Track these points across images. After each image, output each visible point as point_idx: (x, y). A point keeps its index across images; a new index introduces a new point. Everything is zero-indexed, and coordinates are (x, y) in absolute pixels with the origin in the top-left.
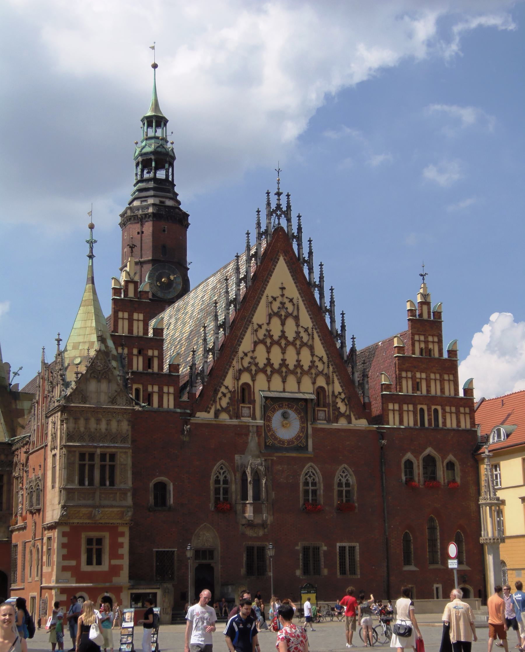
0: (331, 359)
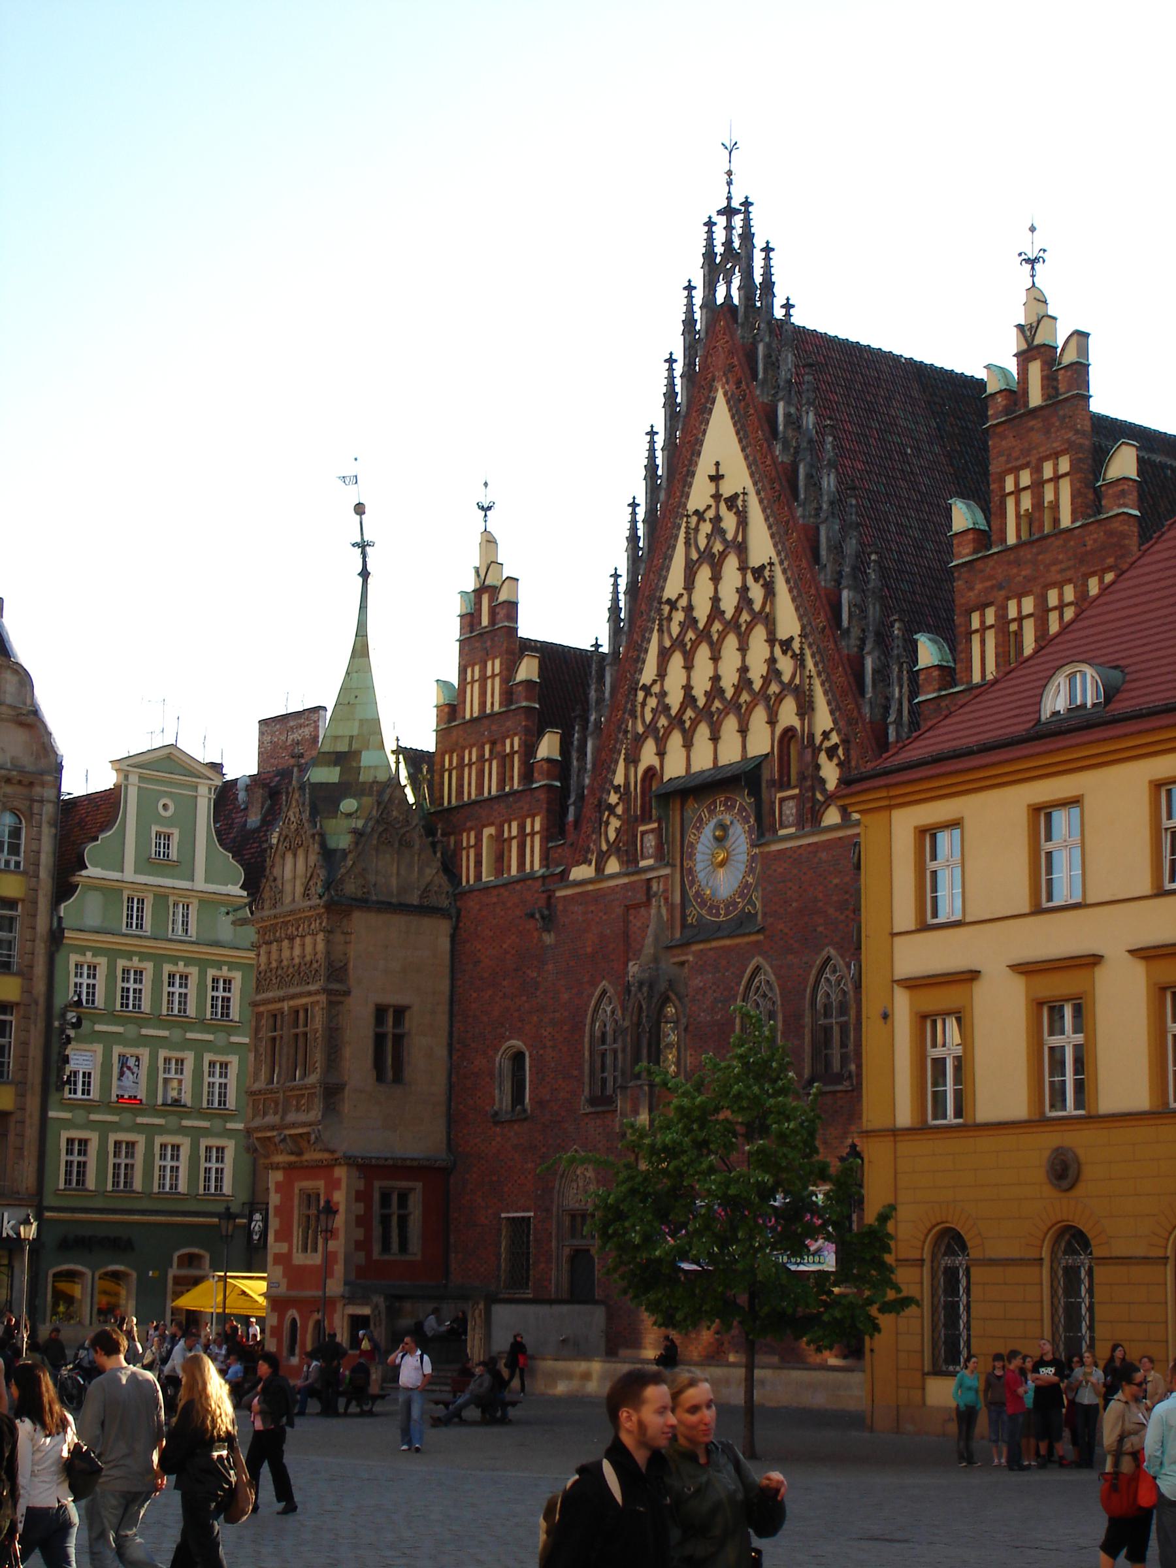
0: (811, 640)
